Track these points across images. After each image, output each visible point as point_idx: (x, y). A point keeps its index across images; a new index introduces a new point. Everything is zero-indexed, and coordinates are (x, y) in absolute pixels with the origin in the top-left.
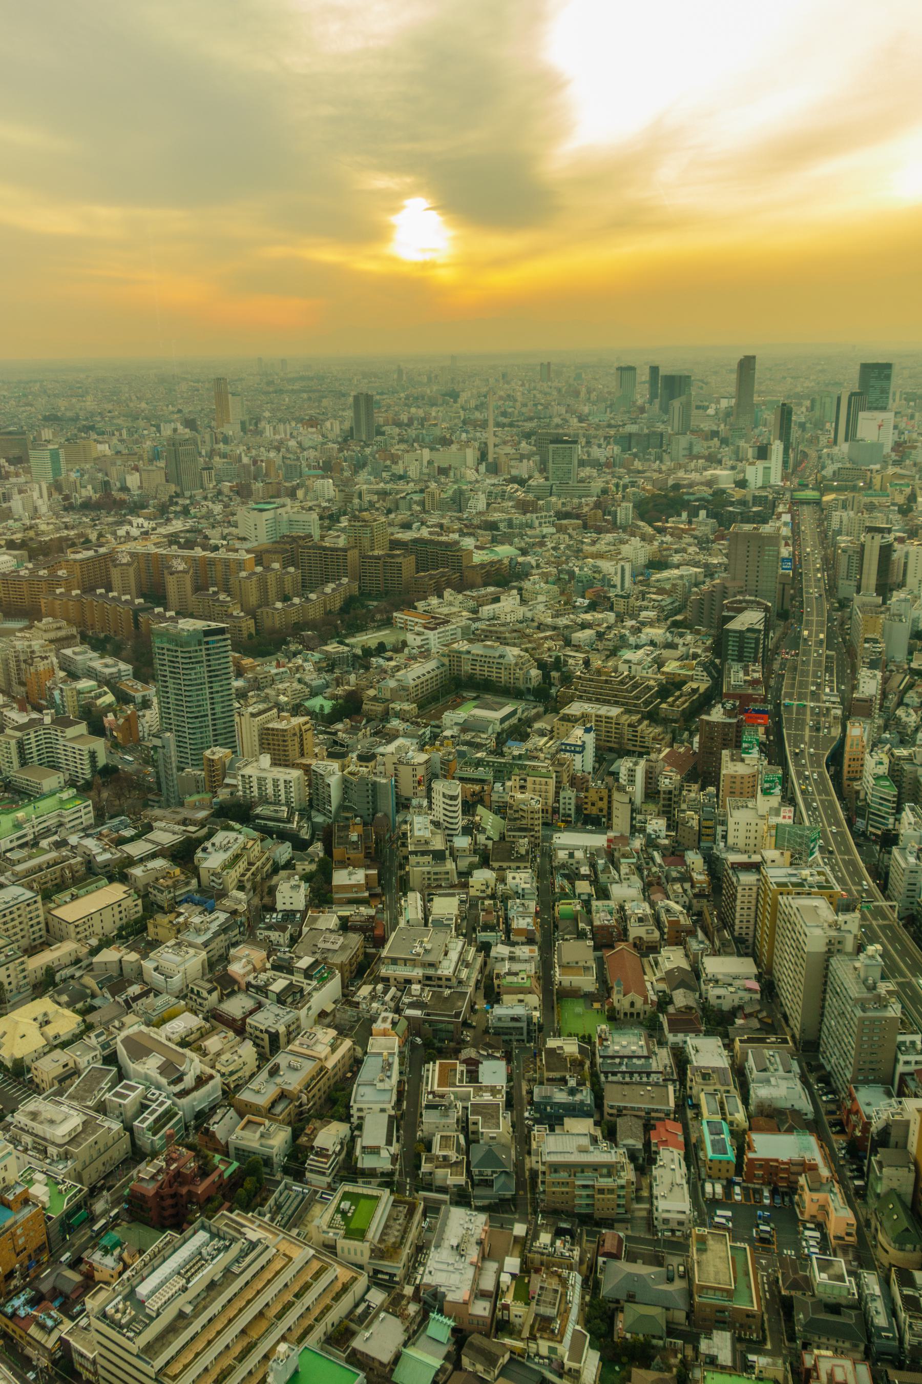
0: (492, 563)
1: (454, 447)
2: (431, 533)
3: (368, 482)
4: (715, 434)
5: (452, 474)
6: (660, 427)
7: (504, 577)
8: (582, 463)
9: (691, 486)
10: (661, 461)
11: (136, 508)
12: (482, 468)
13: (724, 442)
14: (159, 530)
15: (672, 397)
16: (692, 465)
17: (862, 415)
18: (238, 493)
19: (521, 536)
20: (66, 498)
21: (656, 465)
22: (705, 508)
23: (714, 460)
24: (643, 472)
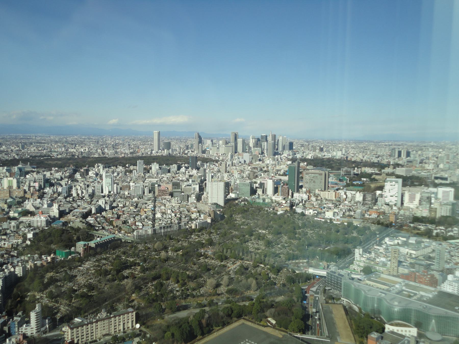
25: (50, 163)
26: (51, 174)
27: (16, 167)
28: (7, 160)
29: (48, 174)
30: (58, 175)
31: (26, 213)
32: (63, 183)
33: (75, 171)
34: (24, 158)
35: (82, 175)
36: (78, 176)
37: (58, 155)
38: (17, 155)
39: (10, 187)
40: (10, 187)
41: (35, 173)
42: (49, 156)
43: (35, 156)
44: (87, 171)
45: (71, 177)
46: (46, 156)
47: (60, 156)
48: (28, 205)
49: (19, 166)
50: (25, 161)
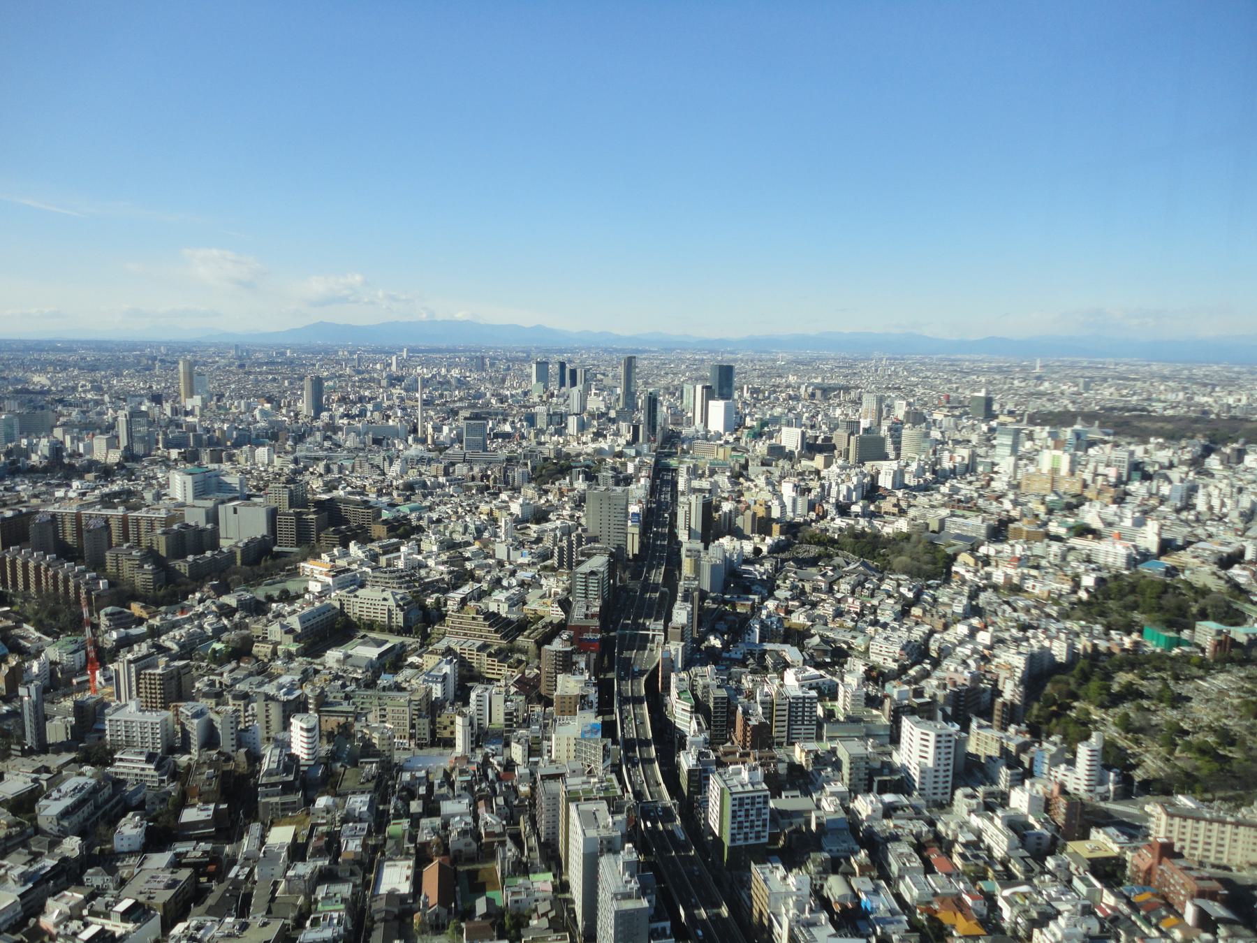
0: (395, 519)
1: (391, 422)
2: (350, 493)
3: (308, 449)
4: (603, 415)
5: (384, 442)
6: (563, 409)
7: (403, 530)
8: (497, 436)
9: (579, 455)
10: (560, 435)
11: (79, 473)
12: (410, 439)
13: (613, 421)
14: (97, 492)
15: (574, 384)
16: (584, 439)
17: (711, 403)
18: (185, 459)
19: (431, 494)
20: (13, 463)
21: (555, 438)
22: (584, 472)
23: (598, 435)
24: (544, 444)
25: (1146, 428)
26: (1146, 451)
27: (1069, 430)
28: (1051, 413)
29: (1139, 451)
30: (1164, 456)
31: (1083, 531)
32: (1175, 475)
33: (1208, 451)
34: (1086, 410)
35: (1226, 462)
36: (1213, 462)
37: (1165, 409)
38: (1073, 402)
39: (1055, 471)
40: (1055, 471)
41: (1109, 446)
42: (1143, 410)
43: (1112, 409)
44: (1240, 454)
45: (1197, 463)
46: (1135, 410)
47: (1170, 412)
48: (1090, 515)
49: (1077, 427)
50: (1089, 418)
